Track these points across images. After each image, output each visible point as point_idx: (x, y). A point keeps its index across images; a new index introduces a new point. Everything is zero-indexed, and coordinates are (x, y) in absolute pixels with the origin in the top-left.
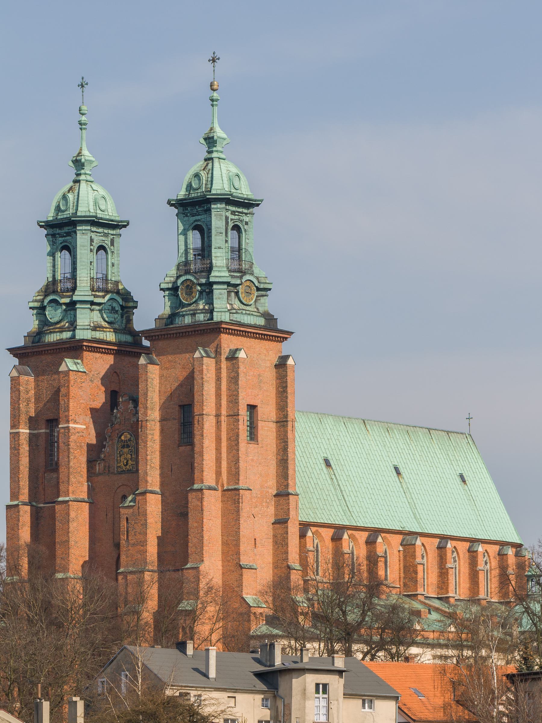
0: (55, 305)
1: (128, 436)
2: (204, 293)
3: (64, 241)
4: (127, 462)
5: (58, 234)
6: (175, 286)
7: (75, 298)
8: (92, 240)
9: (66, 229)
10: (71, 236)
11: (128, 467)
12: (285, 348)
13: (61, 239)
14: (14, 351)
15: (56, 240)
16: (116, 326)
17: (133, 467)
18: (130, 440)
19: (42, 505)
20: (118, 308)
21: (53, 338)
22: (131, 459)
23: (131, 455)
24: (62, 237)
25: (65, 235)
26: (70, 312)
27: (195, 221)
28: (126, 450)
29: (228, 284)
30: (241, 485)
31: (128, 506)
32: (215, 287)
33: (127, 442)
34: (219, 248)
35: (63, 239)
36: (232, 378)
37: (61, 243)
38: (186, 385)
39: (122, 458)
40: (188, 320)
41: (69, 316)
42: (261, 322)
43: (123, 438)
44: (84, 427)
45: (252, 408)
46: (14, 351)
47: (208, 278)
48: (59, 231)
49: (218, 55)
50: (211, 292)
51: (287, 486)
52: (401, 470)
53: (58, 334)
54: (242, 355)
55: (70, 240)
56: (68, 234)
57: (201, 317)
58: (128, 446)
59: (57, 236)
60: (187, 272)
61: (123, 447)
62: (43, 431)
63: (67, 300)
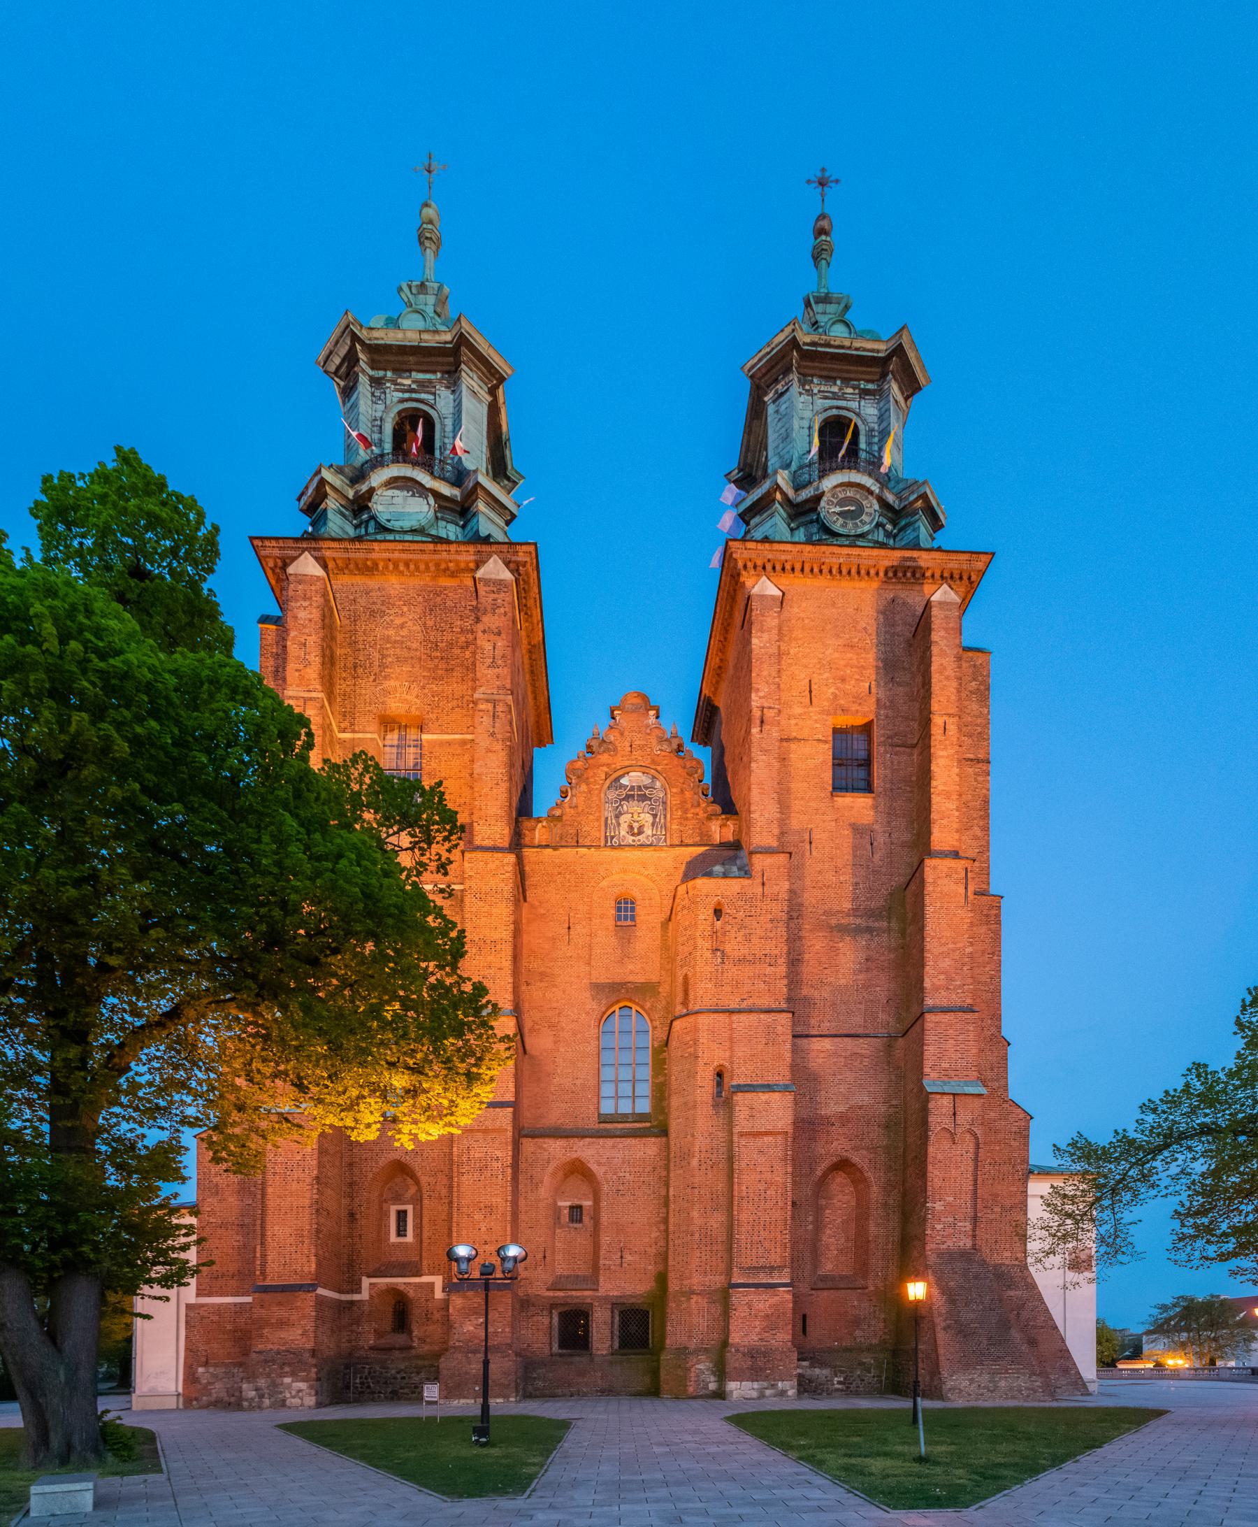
10: (434, 394)
13: (400, 395)
15: (385, 393)
22: (653, 824)
23: (655, 816)
24: (403, 391)
25: (414, 386)
26: (444, 523)
28: (634, 807)
33: (641, 790)
35: (407, 395)
36: (971, 692)
38: (857, 680)
39: (625, 819)
55: (433, 402)
58: (643, 798)
59: (388, 385)
61: (628, 798)
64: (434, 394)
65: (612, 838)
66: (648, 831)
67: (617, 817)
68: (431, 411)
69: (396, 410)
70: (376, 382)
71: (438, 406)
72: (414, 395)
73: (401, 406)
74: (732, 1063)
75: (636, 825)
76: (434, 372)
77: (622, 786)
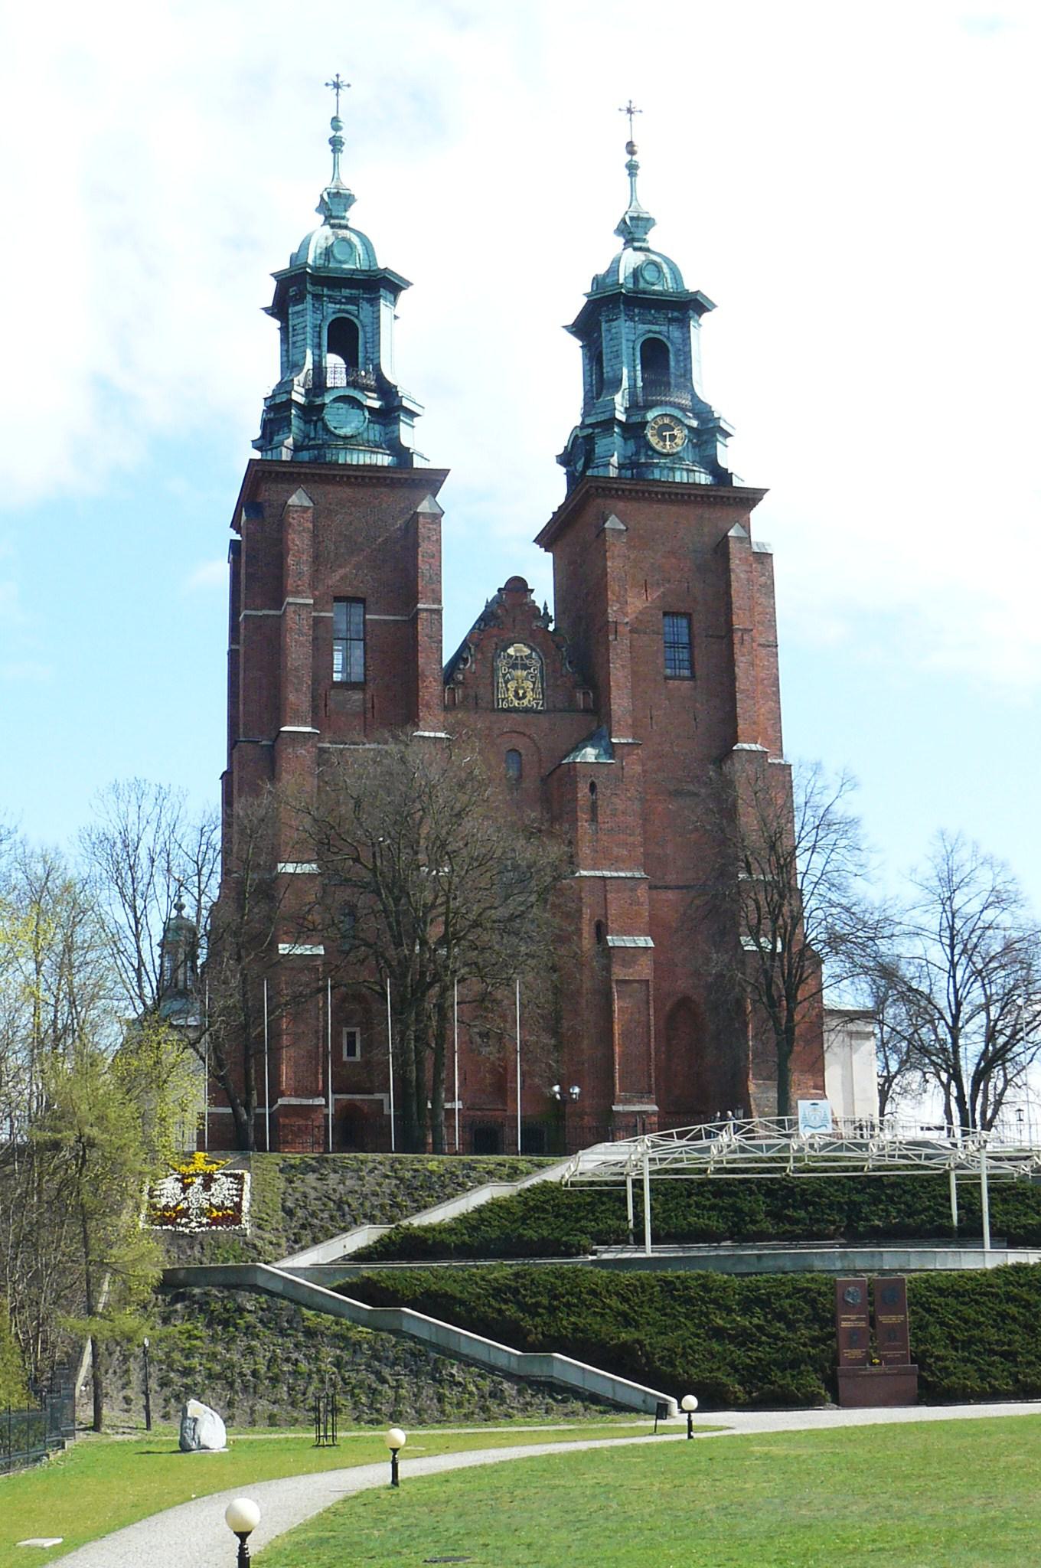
0: (346, 406)
1: (525, 649)
3: (340, 311)
5: (329, 296)
9: (346, 292)
10: (358, 306)
11: (525, 702)
17: (537, 704)
18: (529, 657)
22: (533, 690)
23: (534, 683)
28: (519, 673)
35: (338, 306)
37: (334, 313)
39: (512, 685)
41: (371, 432)
43: (511, 651)
48: (330, 293)
56: (352, 300)
58: (525, 667)
61: (514, 667)
63: (376, 404)
64: (358, 306)
65: (503, 700)
66: (530, 694)
67: (506, 682)
68: (356, 320)
69: (330, 320)
70: (317, 297)
71: (361, 317)
72: (343, 307)
73: (334, 317)
74: (607, 919)
75: (521, 692)
76: (358, 289)
77: (510, 656)
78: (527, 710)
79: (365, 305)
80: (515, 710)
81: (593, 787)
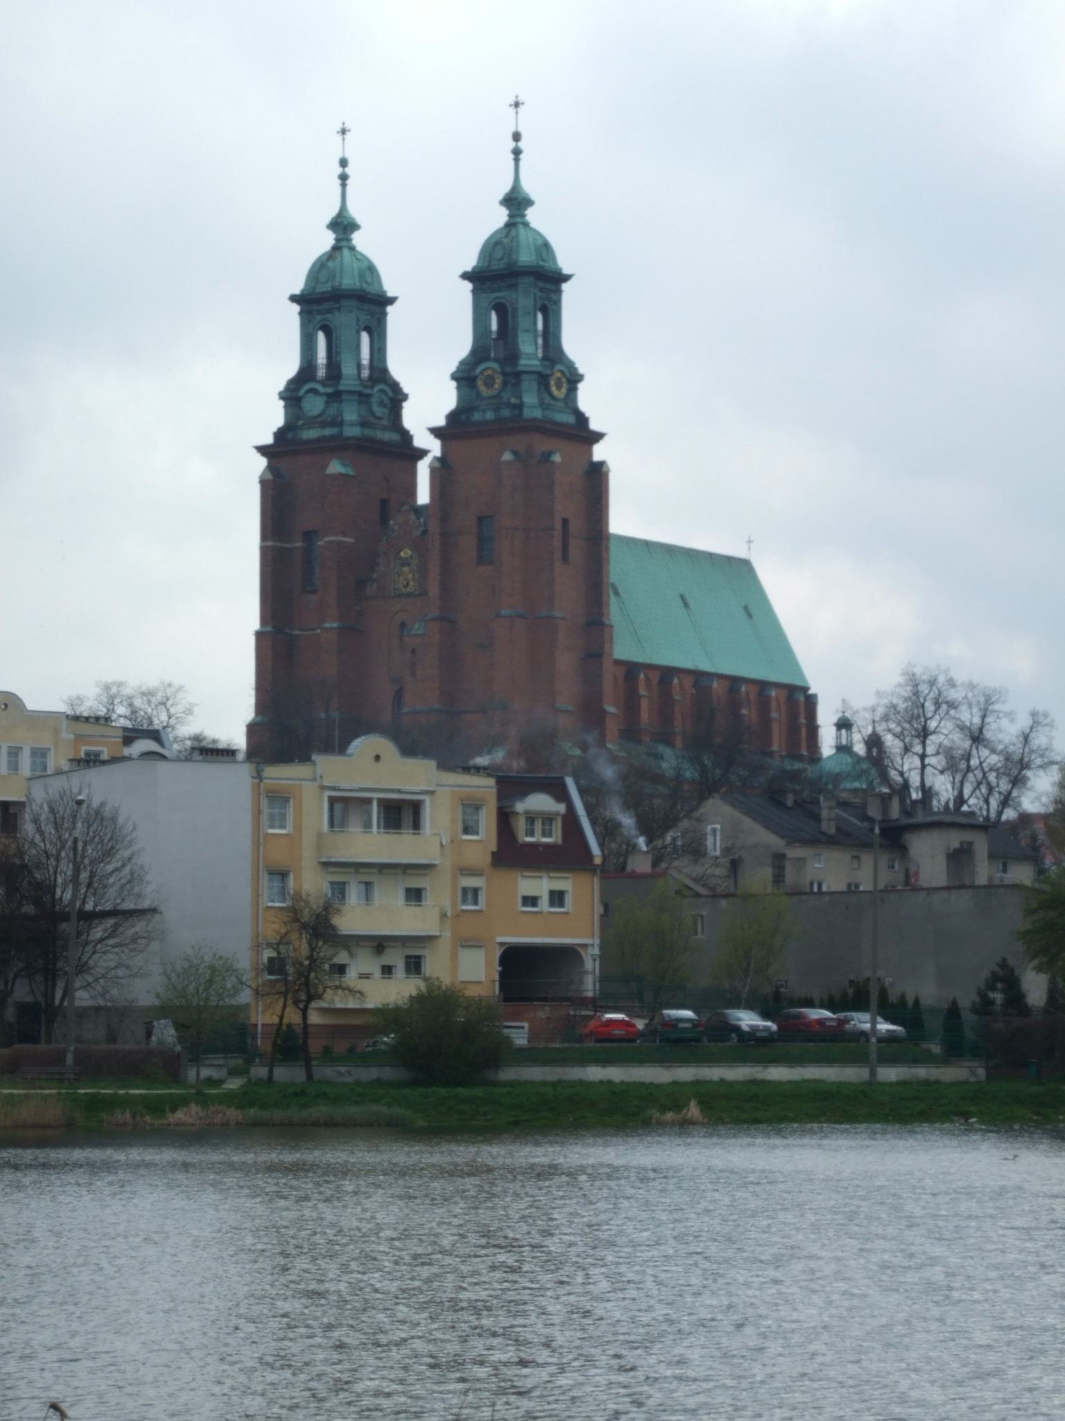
1: (409, 552)
2: (509, 385)
3: (323, 320)
4: (408, 583)
6: (472, 374)
7: (341, 388)
8: (358, 320)
9: (325, 306)
12: (599, 452)
13: (318, 317)
14: (263, 450)
16: (385, 422)
19: (297, 632)
20: (386, 401)
21: (312, 434)
27: (496, 298)
28: (406, 569)
29: (539, 374)
30: (557, 614)
31: (415, 635)
32: (524, 376)
34: (527, 331)
37: (319, 322)
39: (401, 578)
40: (490, 416)
42: (571, 419)
43: (402, 554)
44: (351, 540)
45: (565, 522)
46: (263, 450)
47: (516, 365)
49: (521, 99)
50: (517, 384)
51: (601, 615)
52: (689, 600)
53: (319, 429)
54: (557, 458)
56: (329, 311)
57: (506, 413)
58: (409, 565)
60: (488, 359)
61: (403, 565)
62: (299, 544)
63: (330, 390)
66: (411, 583)
78: (409, 595)
79: (337, 313)
80: (401, 596)
81: (413, 651)
